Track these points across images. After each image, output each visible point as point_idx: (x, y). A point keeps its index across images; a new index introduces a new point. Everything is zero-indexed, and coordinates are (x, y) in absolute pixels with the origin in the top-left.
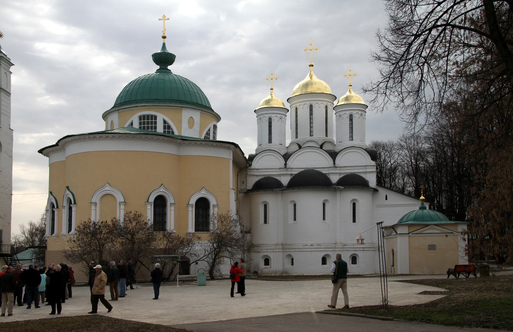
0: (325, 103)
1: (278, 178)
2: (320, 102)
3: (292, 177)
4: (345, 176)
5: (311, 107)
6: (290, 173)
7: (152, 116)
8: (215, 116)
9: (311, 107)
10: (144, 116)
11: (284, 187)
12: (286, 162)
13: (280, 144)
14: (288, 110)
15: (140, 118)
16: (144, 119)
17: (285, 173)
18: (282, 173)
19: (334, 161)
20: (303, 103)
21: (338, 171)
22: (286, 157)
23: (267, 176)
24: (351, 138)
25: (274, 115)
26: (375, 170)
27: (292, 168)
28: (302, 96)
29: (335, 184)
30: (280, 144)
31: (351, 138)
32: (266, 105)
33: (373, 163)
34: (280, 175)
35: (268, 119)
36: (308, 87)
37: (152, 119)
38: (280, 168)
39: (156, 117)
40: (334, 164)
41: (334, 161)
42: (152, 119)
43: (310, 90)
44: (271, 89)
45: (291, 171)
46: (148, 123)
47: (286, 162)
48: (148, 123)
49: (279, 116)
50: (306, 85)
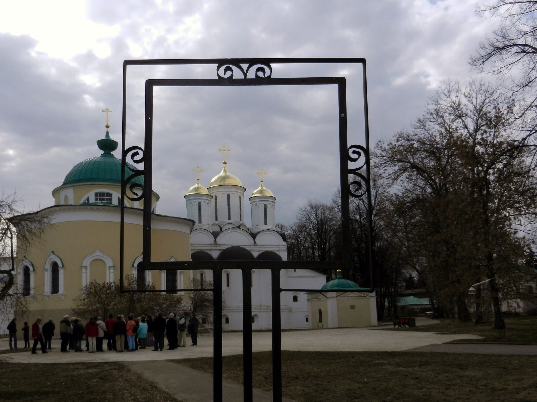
0: (239, 194)
1: (209, 252)
2: (236, 193)
3: (221, 252)
4: (263, 252)
5: (229, 196)
6: (219, 248)
7: (107, 194)
8: (156, 197)
9: (229, 196)
10: (100, 193)
11: (215, 259)
12: (215, 239)
13: (208, 225)
14: (213, 197)
15: (96, 194)
16: (100, 195)
17: (215, 248)
18: (212, 248)
19: (254, 240)
20: (222, 193)
21: (257, 249)
22: (215, 235)
23: (200, 250)
24: (266, 223)
25: (203, 201)
26: (286, 249)
27: (220, 245)
28: (221, 187)
29: (256, 259)
30: (208, 225)
31: (266, 223)
32: (195, 192)
33: (285, 243)
34: (210, 250)
35: (198, 203)
36: (225, 180)
37: (107, 196)
38: (210, 244)
39: (111, 195)
40: (255, 242)
41: (254, 240)
42: (107, 196)
43: (227, 182)
44: (198, 179)
45: (220, 247)
46: (104, 199)
47: (215, 239)
48: (104, 199)
49: (207, 201)
50: (224, 178)
